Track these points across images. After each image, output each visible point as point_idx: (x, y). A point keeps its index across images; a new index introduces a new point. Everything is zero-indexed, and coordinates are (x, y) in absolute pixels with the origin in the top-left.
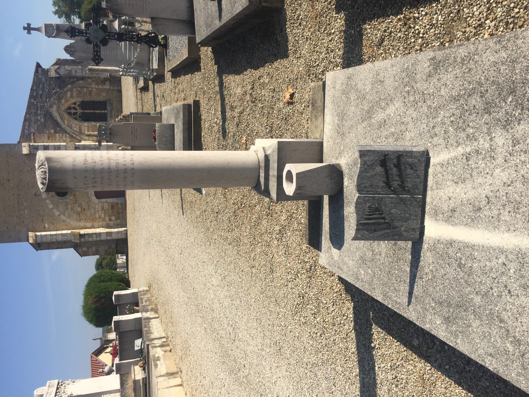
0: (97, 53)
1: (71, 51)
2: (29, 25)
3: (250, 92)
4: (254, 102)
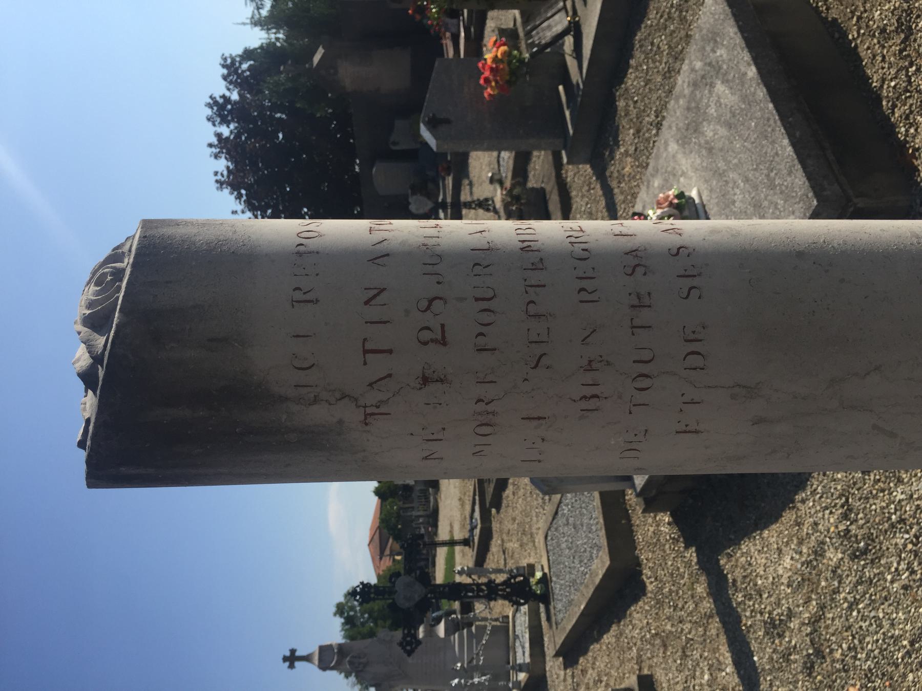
2: (293, 651)
3: (842, 527)
4: (865, 552)
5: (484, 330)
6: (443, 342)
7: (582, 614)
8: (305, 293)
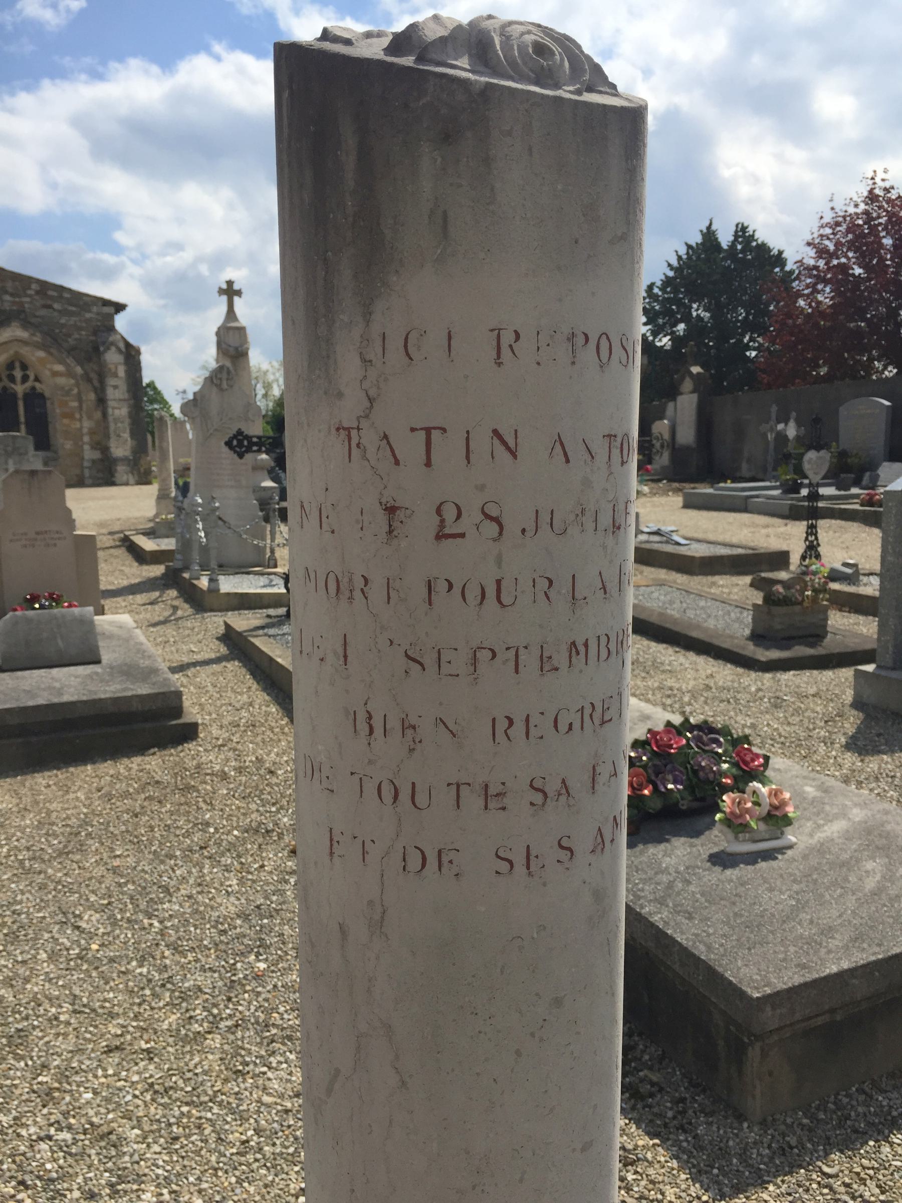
0: (255, 444)
1: (221, 379)
2: (239, 293)
5: (457, 590)
6: (441, 536)
7: (271, 659)
8: (511, 346)
